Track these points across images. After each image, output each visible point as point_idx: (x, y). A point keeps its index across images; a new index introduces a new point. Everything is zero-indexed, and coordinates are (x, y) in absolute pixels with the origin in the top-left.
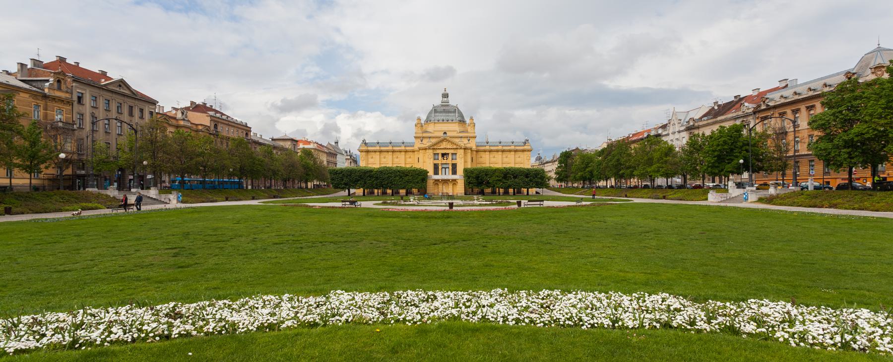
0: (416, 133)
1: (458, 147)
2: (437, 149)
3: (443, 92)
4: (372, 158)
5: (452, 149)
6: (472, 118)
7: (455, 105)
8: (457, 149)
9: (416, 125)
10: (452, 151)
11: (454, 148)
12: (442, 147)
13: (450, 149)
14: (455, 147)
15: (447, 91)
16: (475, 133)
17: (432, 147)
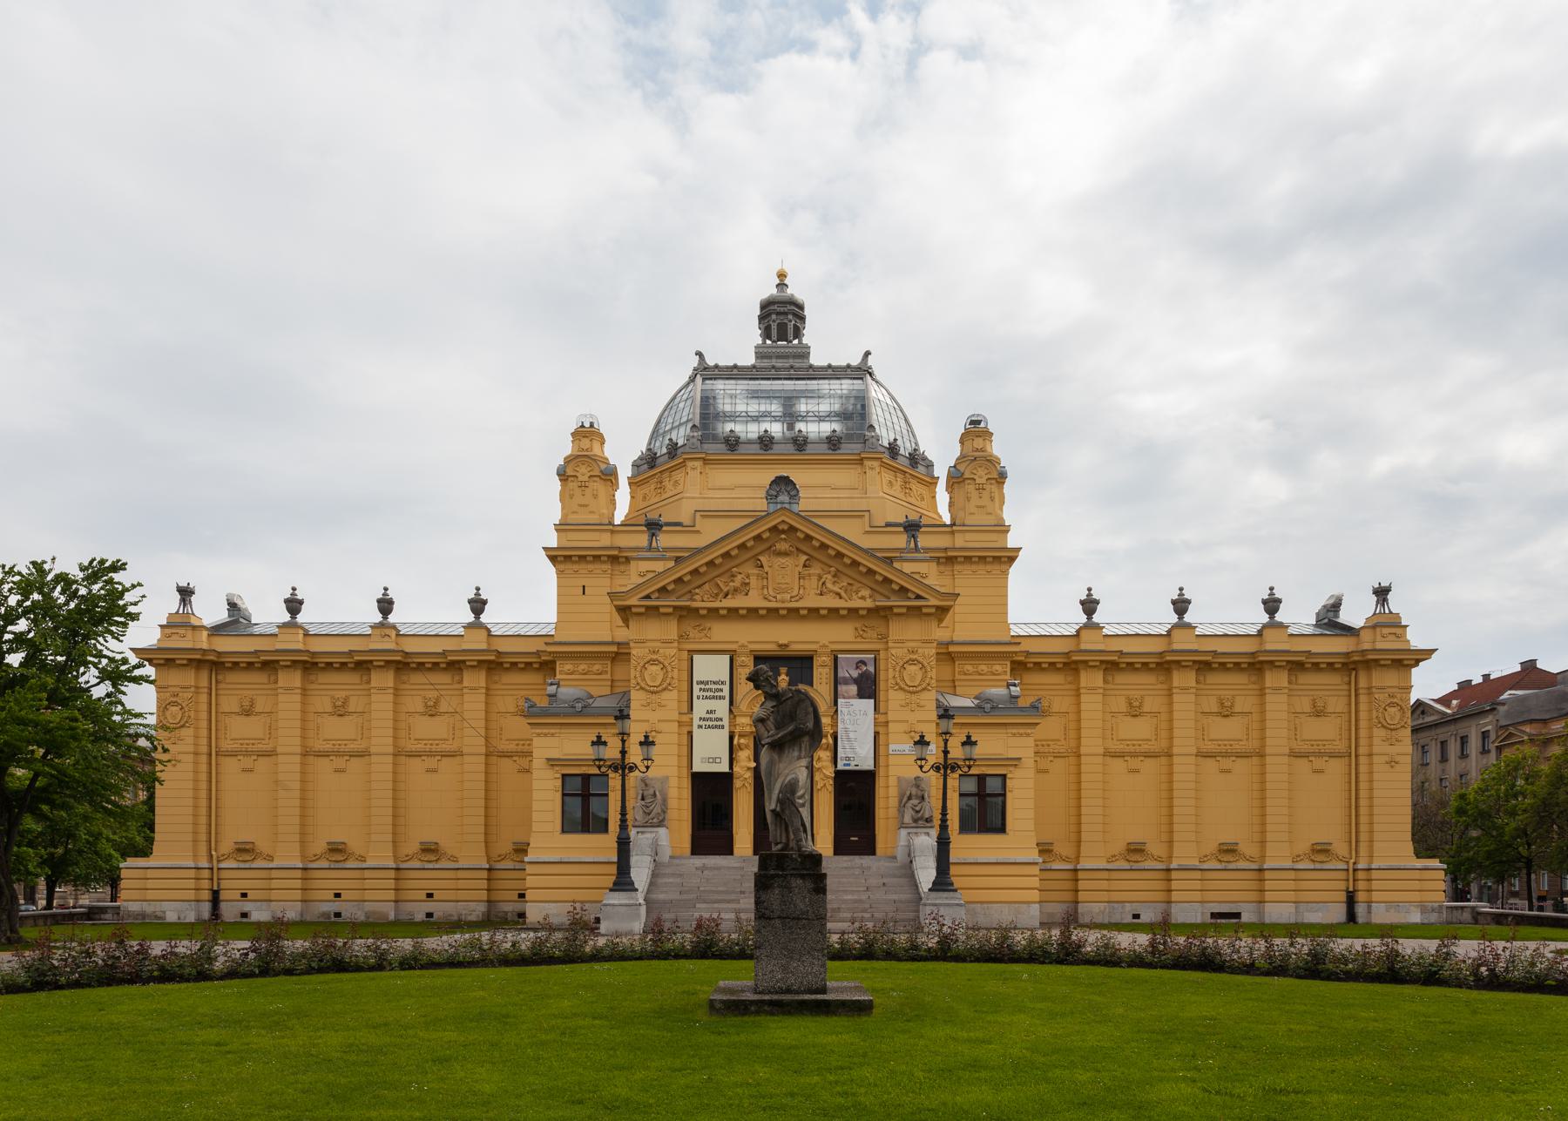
0: (561, 528)
1: (894, 602)
2: (713, 612)
3: (770, 291)
4: (247, 712)
5: (834, 613)
6: (976, 430)
7: (855, 362)
8: (881, 614)
9: (563, 475)
10: (838, 635)
11: (853, 612)
12: (754, 600)
13: (814, 613)
14: (863, 600)
15: (795, 290)
16: (1004, 530)
17: (673, 601)
